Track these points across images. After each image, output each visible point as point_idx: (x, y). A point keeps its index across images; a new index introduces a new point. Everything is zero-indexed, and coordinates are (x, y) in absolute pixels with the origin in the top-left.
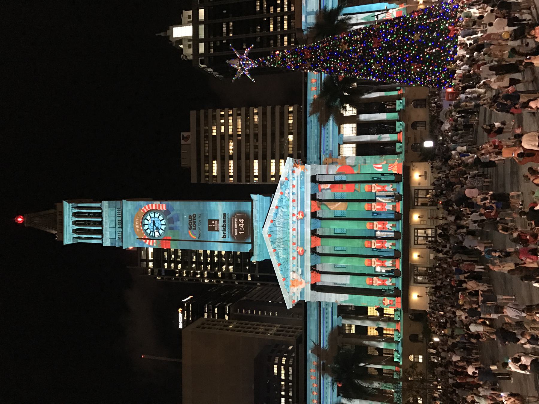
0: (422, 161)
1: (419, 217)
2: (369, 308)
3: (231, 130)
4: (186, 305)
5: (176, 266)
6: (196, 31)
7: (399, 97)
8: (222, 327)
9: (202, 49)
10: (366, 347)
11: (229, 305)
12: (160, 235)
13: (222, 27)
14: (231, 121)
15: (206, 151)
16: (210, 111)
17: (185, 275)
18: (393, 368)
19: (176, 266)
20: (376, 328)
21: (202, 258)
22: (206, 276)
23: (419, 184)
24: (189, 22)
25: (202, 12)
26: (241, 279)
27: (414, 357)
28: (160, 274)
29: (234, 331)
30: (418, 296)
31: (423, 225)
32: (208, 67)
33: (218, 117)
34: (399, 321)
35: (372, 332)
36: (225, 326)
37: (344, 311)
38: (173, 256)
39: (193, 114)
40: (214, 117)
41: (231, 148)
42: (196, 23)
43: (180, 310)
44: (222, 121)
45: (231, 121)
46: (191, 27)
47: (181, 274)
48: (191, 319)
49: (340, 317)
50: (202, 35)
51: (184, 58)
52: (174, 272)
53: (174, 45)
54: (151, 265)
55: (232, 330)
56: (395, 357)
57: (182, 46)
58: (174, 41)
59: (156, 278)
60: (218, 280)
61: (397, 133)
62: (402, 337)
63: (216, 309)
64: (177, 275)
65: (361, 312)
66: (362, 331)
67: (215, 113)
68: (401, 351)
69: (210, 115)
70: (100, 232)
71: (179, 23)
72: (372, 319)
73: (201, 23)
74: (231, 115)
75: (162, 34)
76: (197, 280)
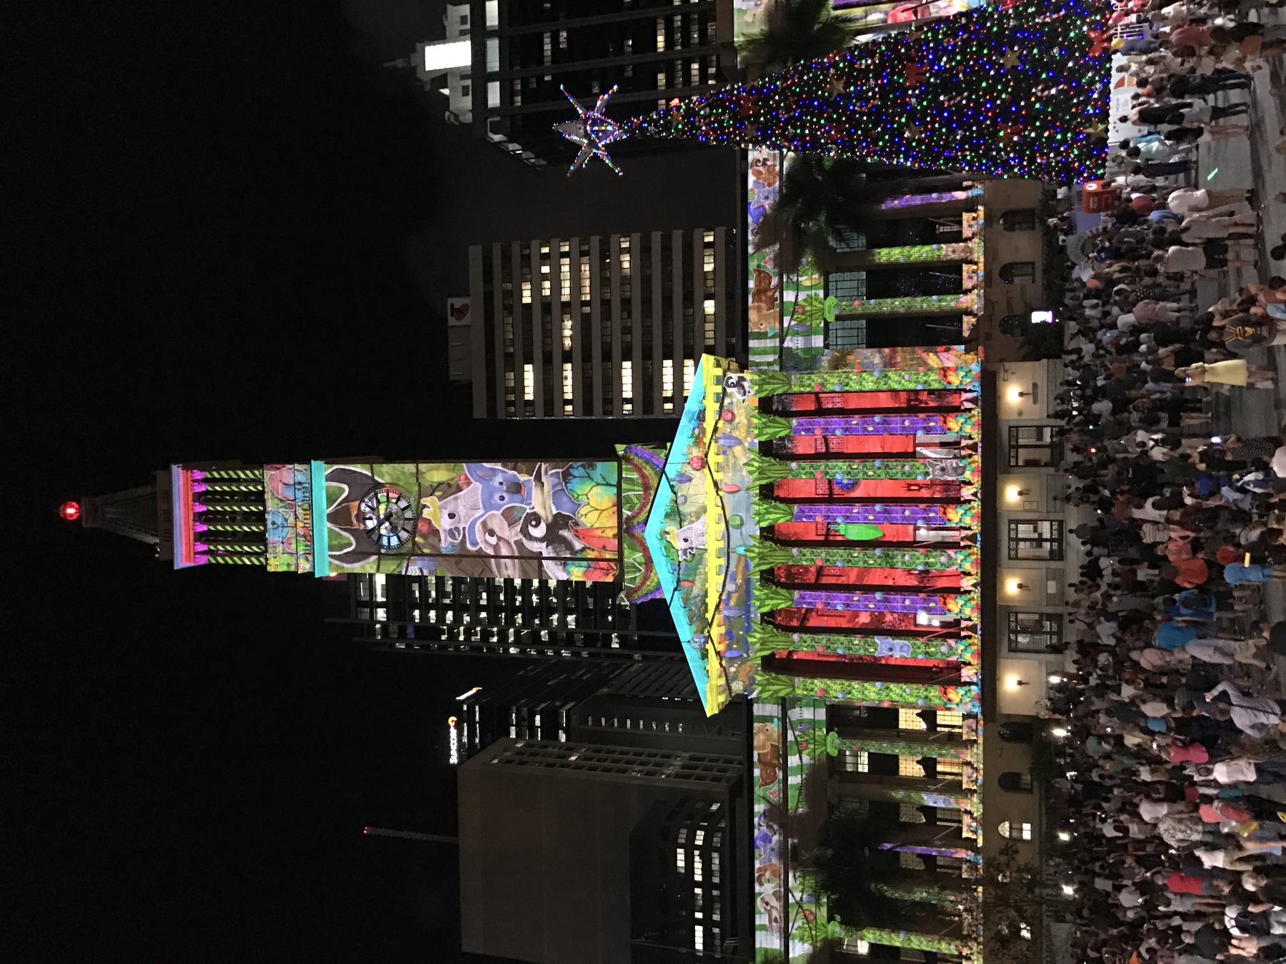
0: (1025, 358)
1: (1020, 493)
2: (902, 711)
3: (566, 291)
4: (465, 708)
5: (441, 618)
6: (479, 54)
7: (970, 205)
8: (551, 760)
10: (895, 806)
11: (568, 706)
13: (542, 45)
14: (566, 269)
15: (508, 343)
16: (516, 247)
17: (462, 638)
18: (962, 854)
19: (441, 618)
20: (919, 758)
21: (502, 597)
22: (511, 639)
23: (1020, 414)
24: (463, 33)
25: (492, 9)
26: (595, 646)
27: (1011, 828)
28: (402, 636)
29: (580, 768)
30: (1020, 683)
31: (1031, 511)
32: (511, 140)
33: (535, 260)
34: (975, 741)
35: (910, 768)
36: (559, 757)
37: (842, 718)
38: (433, 594)
39: (475, 253)
40: (526, 259)
41: (568, 333)
42: (478, 34)
43: (452, 720)
44: (545, 269)
45: (566, 269)
46: (469, 43)
47: (453, 636)
48: (477, 741)
49: (833, 735)
50: (493, 64)
52: (435, 631)
53: (428, 88)
54: (381, 614)
55: (576, 766)
56: (965, 829)
57: (446, 91)
58: (426, 78)
59: (393, 645)
60: (540, 647)
62: (980, 781)
63: (538, 718)
64: (444, 637)
65: (884, 719)
66: (885, 766)
67: (527, 252)
68: (978, 810)
69: (516, 260)
70: (260, 538)
71: (440, 36)
72: (911, 737)
73: (492, 34)
74: (565, 255)
76: (492, 648)
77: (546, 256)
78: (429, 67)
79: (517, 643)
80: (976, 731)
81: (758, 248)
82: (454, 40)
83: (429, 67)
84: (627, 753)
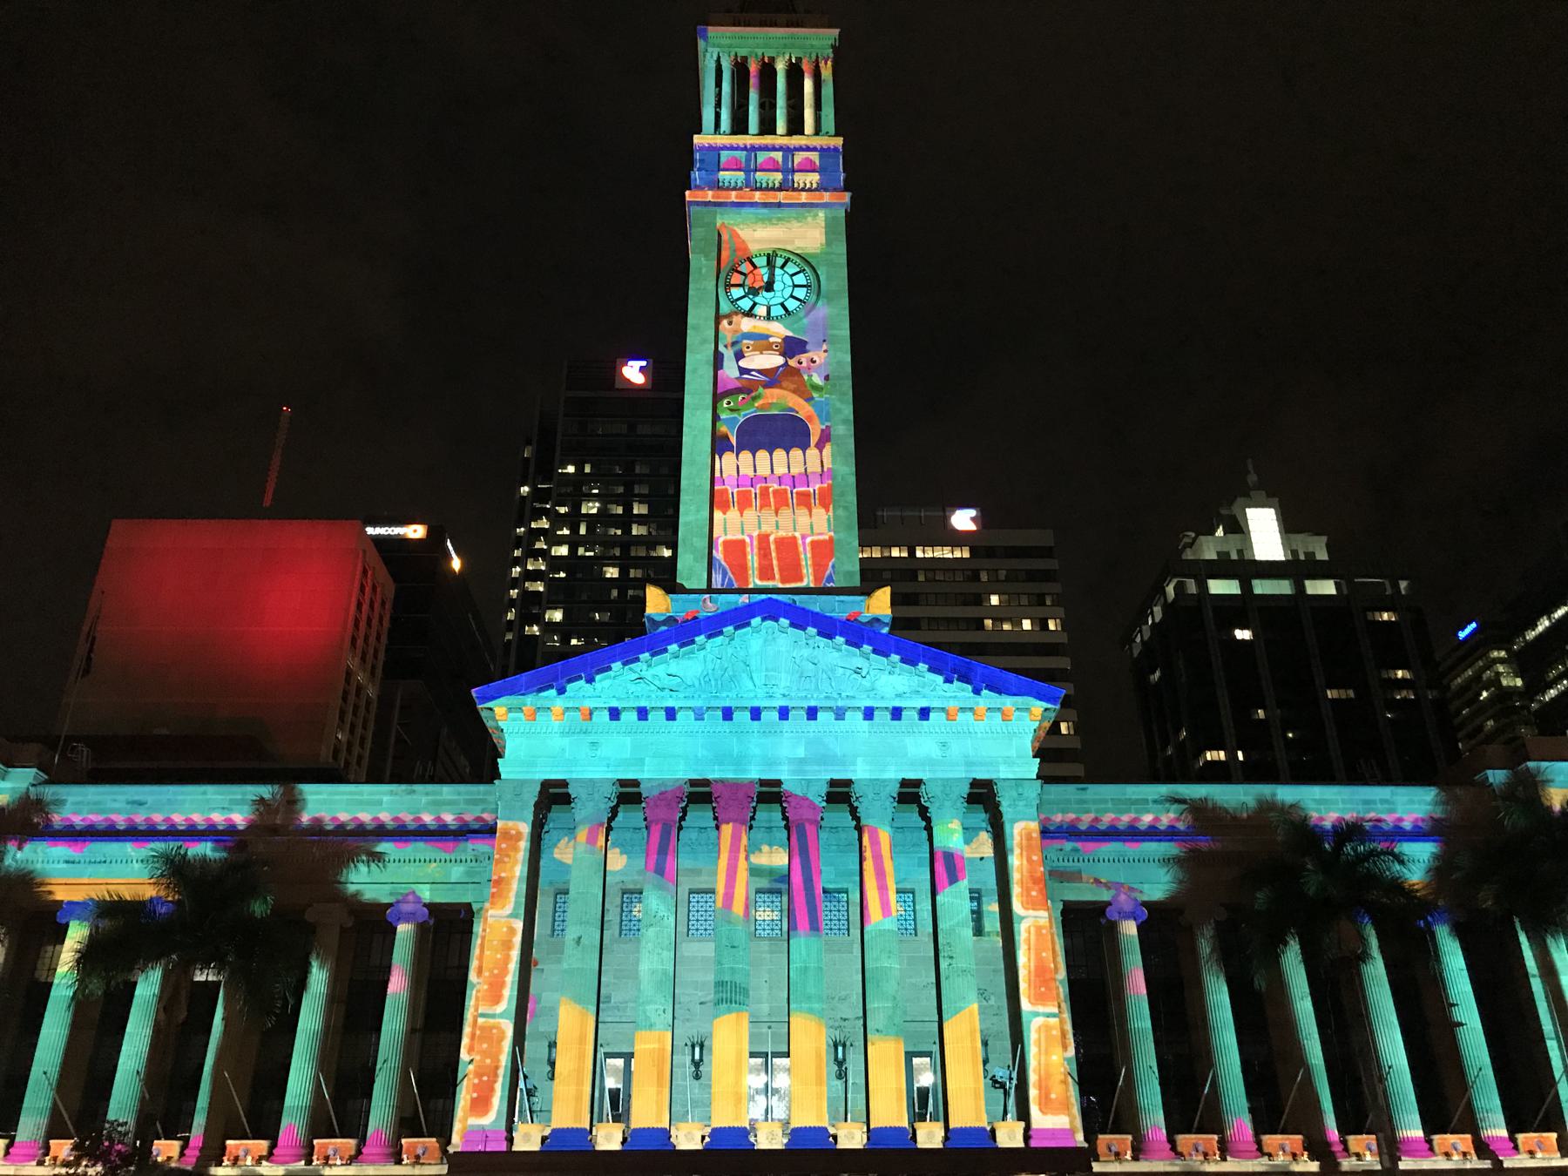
6: (1270, 570)
9: (1217, 587)
12: (734, 302)
15: (930, 575)
16: (1056, 588)
24: (1294, 553)
25: (1327, 588)
29: (348, 681)
32: (1167, 608)
33: (1040, 612)
50: (1261, 587)
51: (1186, 540)
57: (1220, 532)
58: (1235, 510)
60: (516, 627)
61: (1172, 1141)
67: (1048, 602)
71: (1289, 527)
73: (1300, 588)
75: (1252, 478)
77: (1045, 627)
78: (1252, 513)
79: (525, 594)
80: (417, 1161)
81: (1198, 810)
82: (1286, 544)
83: (1249, 511)
84: (362, 745)
